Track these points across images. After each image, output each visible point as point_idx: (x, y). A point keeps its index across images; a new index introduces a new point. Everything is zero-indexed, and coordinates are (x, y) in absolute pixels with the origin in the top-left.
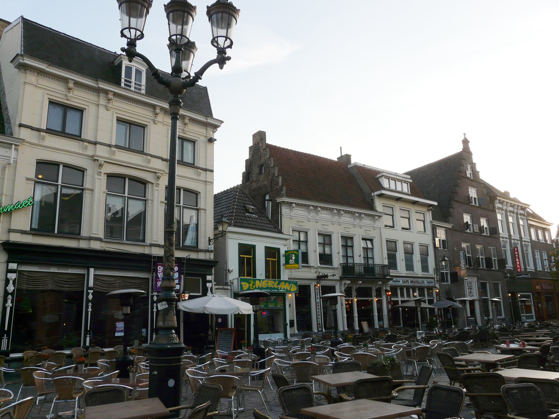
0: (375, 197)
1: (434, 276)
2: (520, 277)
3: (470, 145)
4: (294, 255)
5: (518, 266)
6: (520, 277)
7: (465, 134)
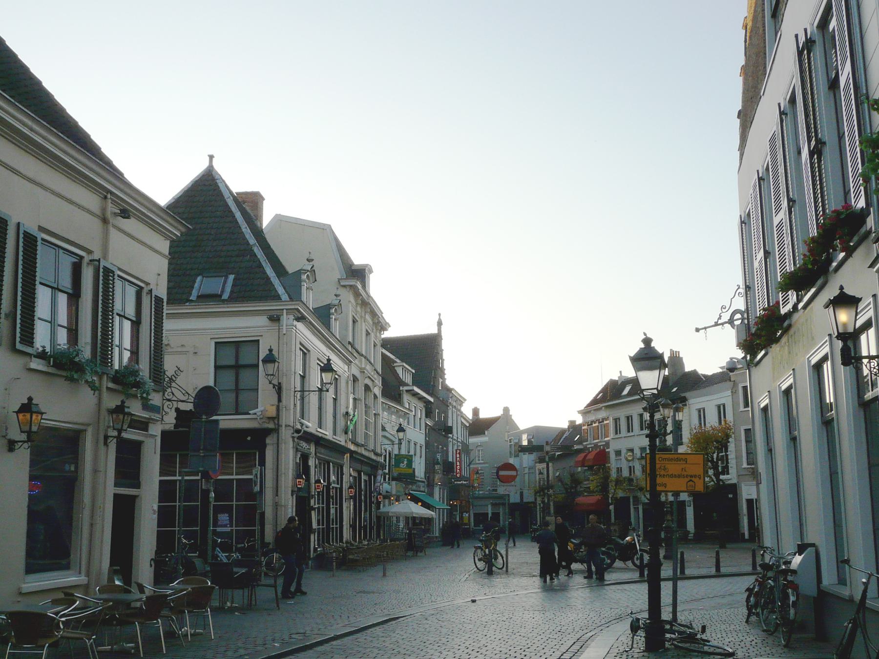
0: (404, 391)
1: (424, 480)
2: (459, 482)
3: (444, 328)
4: (406, 460)
5: (458, 471)
6: (459, 482)
7: (440, 315)
